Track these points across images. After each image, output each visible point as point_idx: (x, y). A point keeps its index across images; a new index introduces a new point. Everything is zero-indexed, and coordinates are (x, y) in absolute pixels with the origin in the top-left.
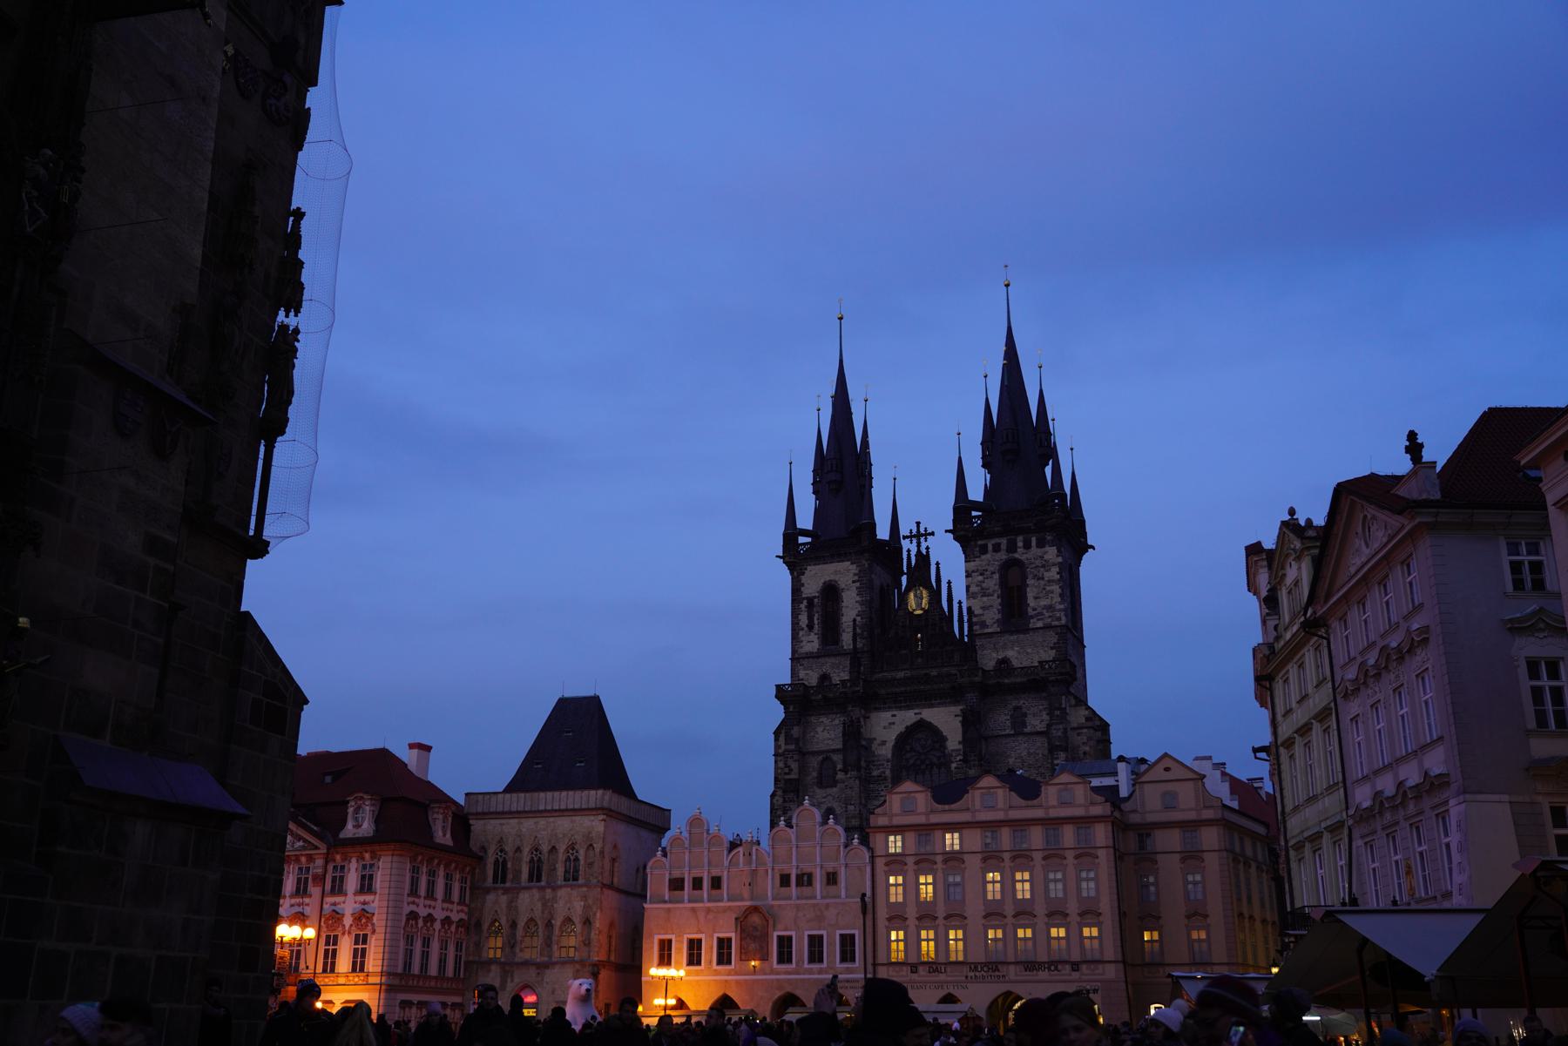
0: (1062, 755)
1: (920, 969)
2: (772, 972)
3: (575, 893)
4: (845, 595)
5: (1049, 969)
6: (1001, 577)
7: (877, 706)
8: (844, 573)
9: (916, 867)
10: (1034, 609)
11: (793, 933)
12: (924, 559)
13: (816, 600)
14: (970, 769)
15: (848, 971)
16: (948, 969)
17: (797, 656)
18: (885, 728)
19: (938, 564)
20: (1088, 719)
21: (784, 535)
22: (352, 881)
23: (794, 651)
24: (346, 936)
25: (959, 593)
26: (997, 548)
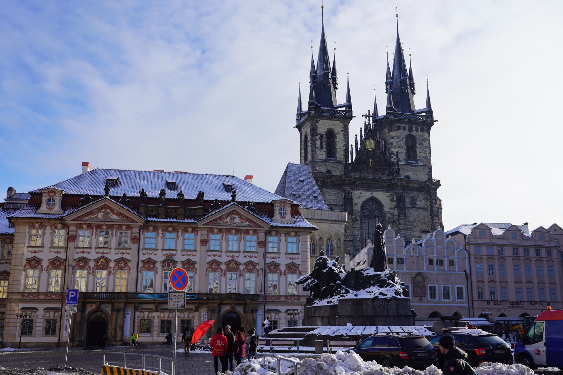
0: (437, 219)
1: (491, 303)
2: (428, 302)
4: (337, 136)
5: (539, 304)
7: (353, 188)
8: (336, 126)
9: (487, 261)
10: (419, 157)
11: (436, 286)
13: (324, 136)
14: (401, 220)
16: (502, 303)
18: (357, 198)
21: (308, 103)
23: (313, 158)
24: (283, 275)
26: (404, 129)
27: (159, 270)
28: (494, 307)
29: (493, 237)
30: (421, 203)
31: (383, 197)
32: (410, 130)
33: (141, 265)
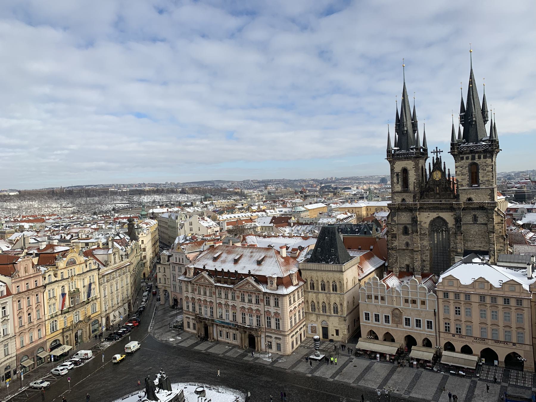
0: (492, 235)
1: (456, 336)
2: (404, 328)
3: (336, 295)
5: (504, 343)
6: (469, 169)
8: (409, 165)
10: (482, 181)
12: (439, 161)
13: (400, 173)
15: (430, 332)
17: (393, 192)
19: (444, 162)
20: (502, 220)
22: (272, 302)
25: (453, 172)
27: (224, 308)
28: (459, 339)
29: (460, 286)
30: (482, 219)
31: (448, 217)
32: (473, 158)
33: (217, 305)
